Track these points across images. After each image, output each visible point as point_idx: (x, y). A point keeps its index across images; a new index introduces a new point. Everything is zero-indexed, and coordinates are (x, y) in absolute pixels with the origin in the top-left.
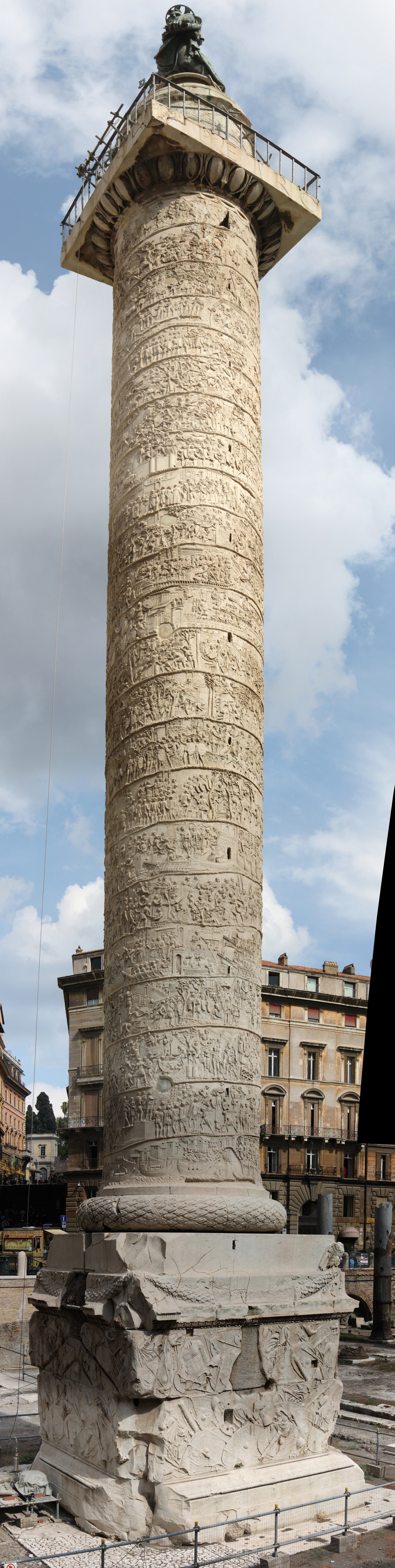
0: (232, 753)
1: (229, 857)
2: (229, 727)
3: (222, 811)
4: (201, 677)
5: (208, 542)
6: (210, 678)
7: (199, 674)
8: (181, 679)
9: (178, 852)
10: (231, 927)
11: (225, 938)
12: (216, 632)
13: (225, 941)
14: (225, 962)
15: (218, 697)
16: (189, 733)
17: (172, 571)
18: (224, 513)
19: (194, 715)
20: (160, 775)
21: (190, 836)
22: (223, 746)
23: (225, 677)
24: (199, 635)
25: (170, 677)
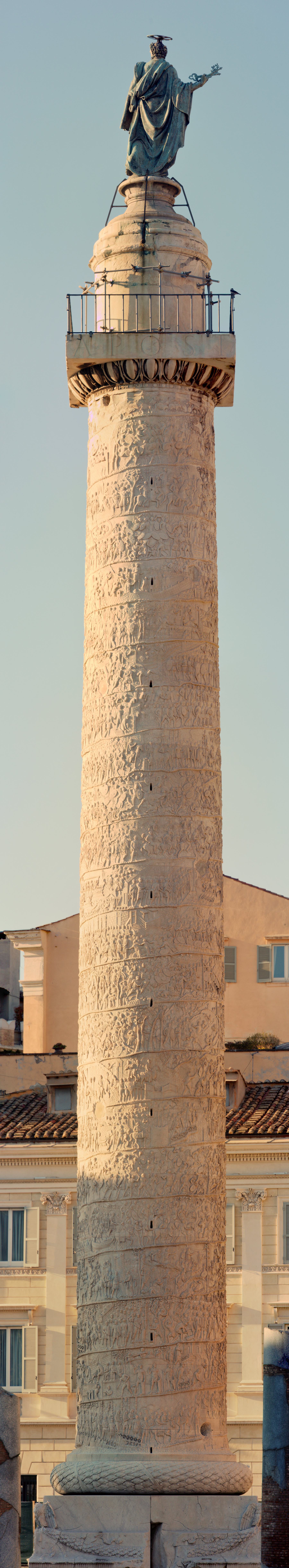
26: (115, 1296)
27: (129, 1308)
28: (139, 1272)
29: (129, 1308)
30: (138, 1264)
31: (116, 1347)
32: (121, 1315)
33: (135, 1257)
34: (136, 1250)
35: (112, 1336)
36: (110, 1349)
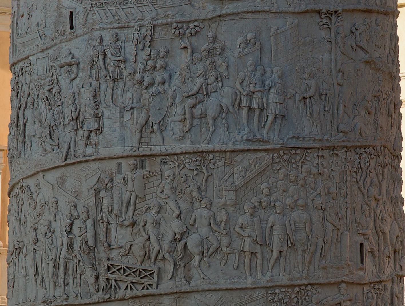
26: (274, 136)
27: (314, 170)
28: (334, 73)
29: (314, 170)
30: (330, 52)
31: (283, 279)
32: (292, 188)
33: (323, 33)
34: (329, 14)
35: (271, 244)
36: (263, 281)
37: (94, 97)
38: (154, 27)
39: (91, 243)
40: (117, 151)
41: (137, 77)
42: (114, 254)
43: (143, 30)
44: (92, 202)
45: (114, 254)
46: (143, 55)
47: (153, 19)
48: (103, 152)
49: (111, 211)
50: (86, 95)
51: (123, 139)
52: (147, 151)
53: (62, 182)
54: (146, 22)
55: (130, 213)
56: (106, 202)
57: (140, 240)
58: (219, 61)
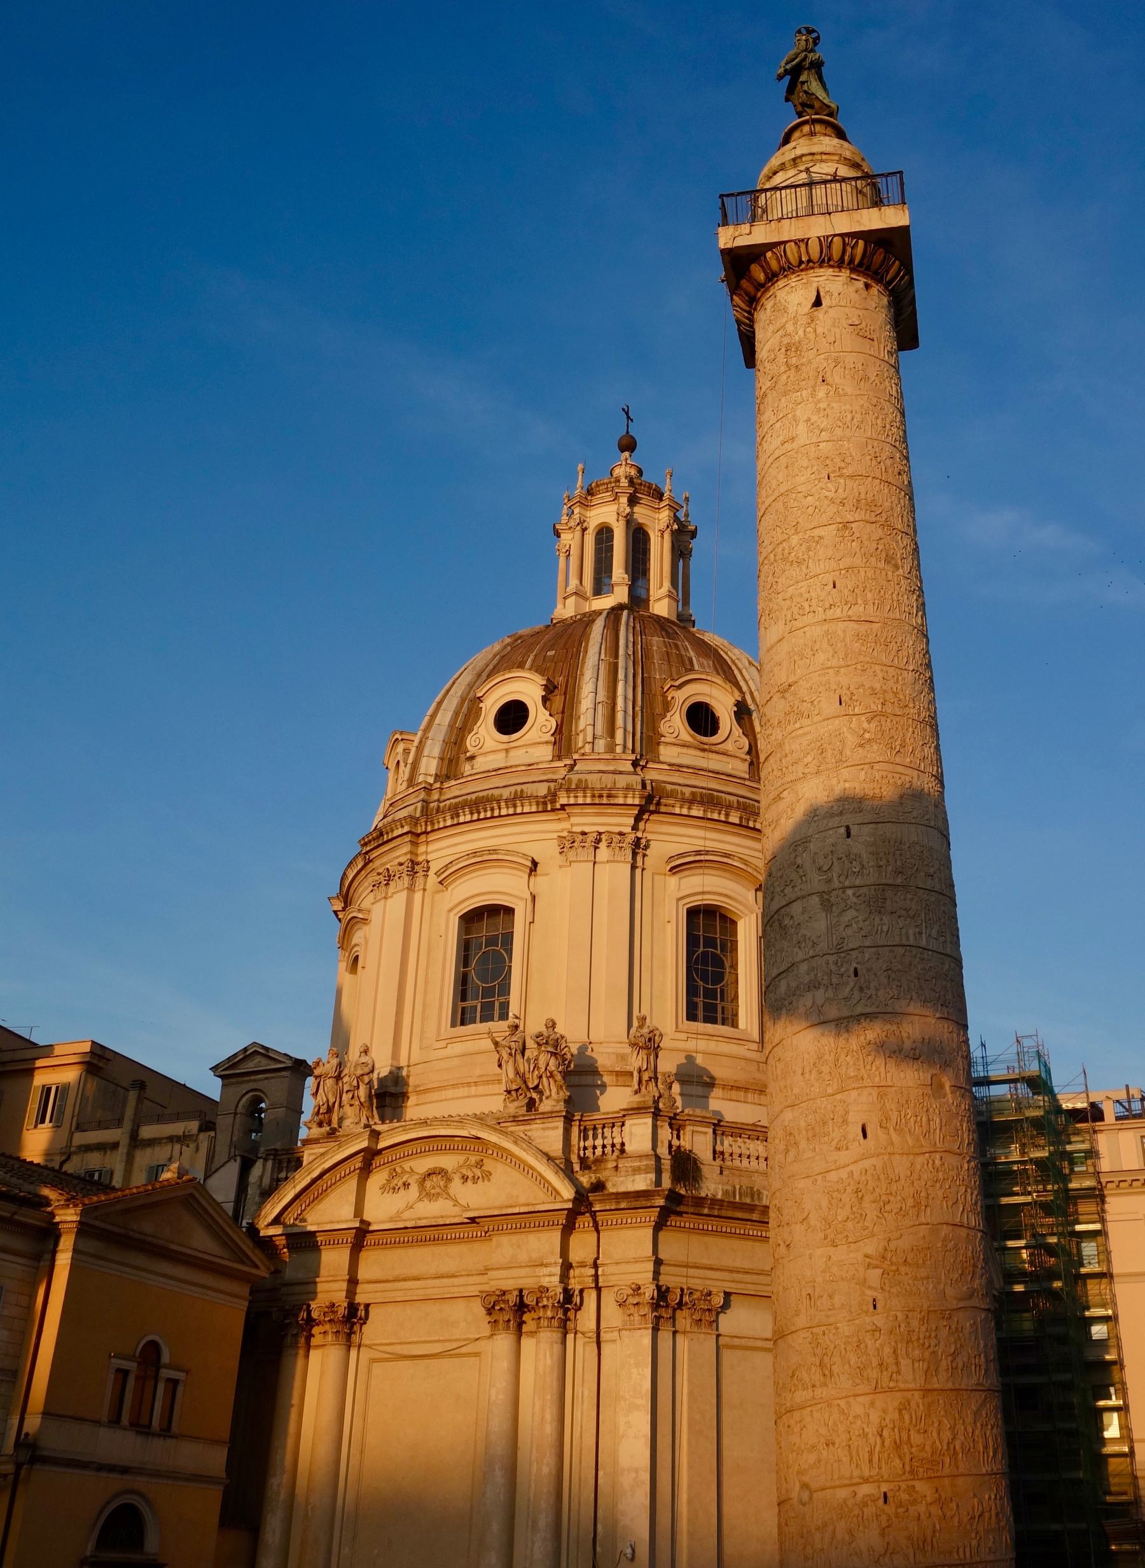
0: (861, 989)
1: (865, 1136)
2: (854, 954)
3: (852, 1074)
4: (815, 900)
5: (815, 719)
6: (826, 897)
7: (814, 896)
8: (796, 908)
9: (803, 1144)
10: (875, 1238)
11: (866, 1256)
12: (831, 832)
13: (868, 1260)
14: (868, 1292)
15: (835, 920)
16: (807, 979)
17: (784, 769)
18: (831, 671)
19: (811, 953)
20: (784, 1042)
21: (813, 1122)
22: (847, 983)
23: (844, 888)
24: (812, 846)
25: (787, 909)
37: (894, 1352)
38: (929, 1312)
39: (898, 1442)
40: (912, 1386)
41: (921, 1341)
42: (913, 1450)
43: (923, 1313)
44: (896, 1416)
45: (913, 1450)
46: (923, 1329)
47: (929, 1307)
48: (902, 1386)
49: (911, 1423)
50: (887, 1350)
51: (915, 1379)
52: (929, 1387)
53: (872, 1404)
54: (925, 1307)
55: (922, 1425)
56: (907, 1417)
57: (929, 1443)
58: (961, 1335)
